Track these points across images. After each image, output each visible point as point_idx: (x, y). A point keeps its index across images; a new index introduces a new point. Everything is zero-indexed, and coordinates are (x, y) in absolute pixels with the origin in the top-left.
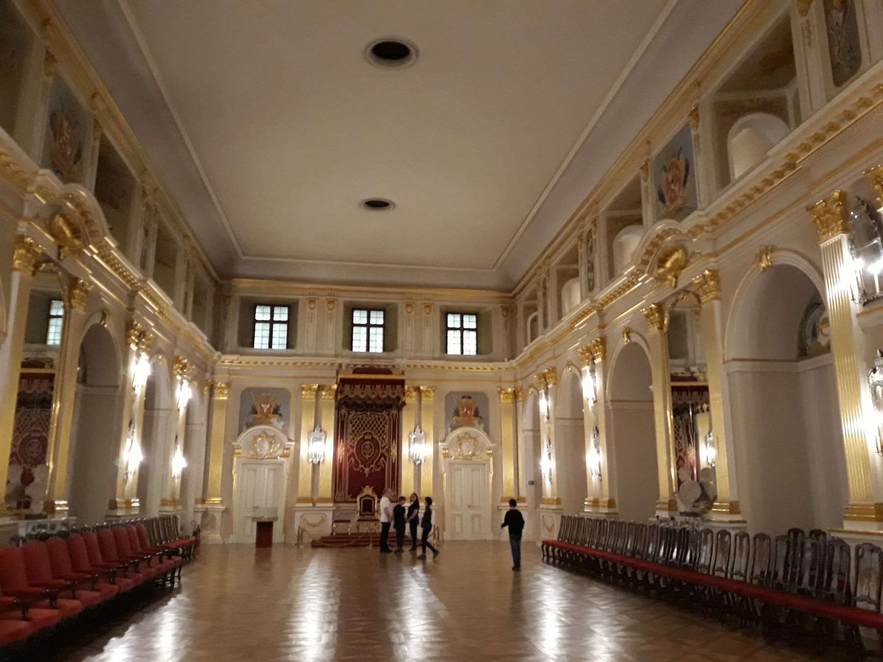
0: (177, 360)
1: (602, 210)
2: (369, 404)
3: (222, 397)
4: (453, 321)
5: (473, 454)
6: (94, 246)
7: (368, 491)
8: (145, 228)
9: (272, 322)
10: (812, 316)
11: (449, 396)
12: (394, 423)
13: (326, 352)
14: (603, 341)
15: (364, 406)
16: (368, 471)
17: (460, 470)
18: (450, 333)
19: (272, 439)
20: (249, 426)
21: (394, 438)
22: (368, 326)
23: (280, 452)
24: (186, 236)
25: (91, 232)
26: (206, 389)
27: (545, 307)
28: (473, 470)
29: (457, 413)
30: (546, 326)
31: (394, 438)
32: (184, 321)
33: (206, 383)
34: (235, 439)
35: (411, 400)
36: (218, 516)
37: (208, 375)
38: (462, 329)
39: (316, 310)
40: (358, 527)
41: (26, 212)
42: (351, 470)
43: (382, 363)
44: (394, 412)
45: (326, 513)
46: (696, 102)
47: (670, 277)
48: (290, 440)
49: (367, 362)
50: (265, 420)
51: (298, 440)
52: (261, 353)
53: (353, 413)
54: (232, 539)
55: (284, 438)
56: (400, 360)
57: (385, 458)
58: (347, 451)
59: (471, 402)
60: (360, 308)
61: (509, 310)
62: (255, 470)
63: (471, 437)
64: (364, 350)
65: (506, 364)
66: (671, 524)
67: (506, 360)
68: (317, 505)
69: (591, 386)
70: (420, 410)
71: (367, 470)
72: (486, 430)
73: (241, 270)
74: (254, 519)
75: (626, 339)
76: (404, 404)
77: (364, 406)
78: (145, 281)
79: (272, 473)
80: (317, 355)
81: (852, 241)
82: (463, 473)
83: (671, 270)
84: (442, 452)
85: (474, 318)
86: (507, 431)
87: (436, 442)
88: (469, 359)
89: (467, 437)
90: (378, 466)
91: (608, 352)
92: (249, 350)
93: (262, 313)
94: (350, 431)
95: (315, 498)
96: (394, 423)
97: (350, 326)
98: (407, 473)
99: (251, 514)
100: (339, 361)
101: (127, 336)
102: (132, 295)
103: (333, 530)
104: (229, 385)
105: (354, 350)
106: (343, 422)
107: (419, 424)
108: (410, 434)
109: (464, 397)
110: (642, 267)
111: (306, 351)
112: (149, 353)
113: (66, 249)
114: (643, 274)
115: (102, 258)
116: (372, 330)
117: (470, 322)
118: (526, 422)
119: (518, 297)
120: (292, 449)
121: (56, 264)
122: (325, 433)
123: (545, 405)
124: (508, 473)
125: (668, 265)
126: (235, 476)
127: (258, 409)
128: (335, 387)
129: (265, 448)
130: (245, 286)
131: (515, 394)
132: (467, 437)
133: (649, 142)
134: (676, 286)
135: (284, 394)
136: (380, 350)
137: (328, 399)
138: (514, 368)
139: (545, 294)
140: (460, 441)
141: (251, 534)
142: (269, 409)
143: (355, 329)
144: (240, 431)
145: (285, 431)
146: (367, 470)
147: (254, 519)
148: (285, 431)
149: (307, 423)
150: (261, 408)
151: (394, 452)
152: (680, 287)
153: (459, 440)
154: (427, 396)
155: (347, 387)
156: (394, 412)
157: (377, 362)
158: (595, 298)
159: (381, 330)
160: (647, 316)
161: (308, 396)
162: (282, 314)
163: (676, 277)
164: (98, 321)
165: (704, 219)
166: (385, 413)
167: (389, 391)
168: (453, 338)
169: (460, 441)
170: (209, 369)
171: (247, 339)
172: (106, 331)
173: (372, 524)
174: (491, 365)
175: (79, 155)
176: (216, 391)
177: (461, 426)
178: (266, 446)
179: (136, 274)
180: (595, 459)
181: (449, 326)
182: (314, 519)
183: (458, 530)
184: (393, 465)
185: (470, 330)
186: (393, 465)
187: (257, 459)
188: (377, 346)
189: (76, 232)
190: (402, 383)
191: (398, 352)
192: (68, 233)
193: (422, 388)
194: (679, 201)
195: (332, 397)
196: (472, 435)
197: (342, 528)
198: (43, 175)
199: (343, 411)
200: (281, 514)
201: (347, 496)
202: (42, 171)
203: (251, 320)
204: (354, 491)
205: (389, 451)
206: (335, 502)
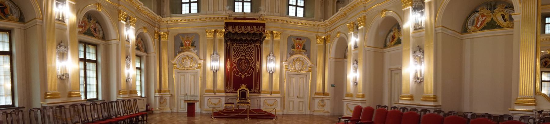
5: (301, 70)
11: (290, 38)
16: (243, 78)
19: (192, 59)
20: (179, 52)
23: (196, 66)
28: (300, 78)
34: (173, 60)
49: (242, 16)
50: (187, 50)
51: (205, 60)
59: (301, 41)
62: (184, 75)
63: (300, 61)
68: (216, 94)
70: (273, 44)
71: (243, 76)
72: (309, 57)
74: (185, 101)
79: (192, 76)
82: (295, 80)
87: (281, 62)
89: (298, 60)
90: (249, 74)
95: (215, 90)
99: (183, 98)
108: (267, 56)
109: (297, 39)
118: (332, 52)
120: (202, 64)
126: (175, 78)
127: (184, 44)
129: (188, 64)
132: (298, 60)
135: (197, 35)
136: (249, 11)
140: (294, 61)
141: (184, 108)
145: (198, 54)
146: (243, 76)
147: (185, 101)
150: (185, 43)
151: (258, 66)
153: (294, 61)
154: (277, 36)
161: (209, 36)
169: (294, 61)
173: (246, 105)
178: (189, 63)
182: (215, 101)
183: (291, 109)
184: (258, 73)
186: (258, 73)
187: (185, 71)
193: (274, 32)
196: (301, 60)
200: (199, 99)
201: (232, 90)
204: (236, 86)
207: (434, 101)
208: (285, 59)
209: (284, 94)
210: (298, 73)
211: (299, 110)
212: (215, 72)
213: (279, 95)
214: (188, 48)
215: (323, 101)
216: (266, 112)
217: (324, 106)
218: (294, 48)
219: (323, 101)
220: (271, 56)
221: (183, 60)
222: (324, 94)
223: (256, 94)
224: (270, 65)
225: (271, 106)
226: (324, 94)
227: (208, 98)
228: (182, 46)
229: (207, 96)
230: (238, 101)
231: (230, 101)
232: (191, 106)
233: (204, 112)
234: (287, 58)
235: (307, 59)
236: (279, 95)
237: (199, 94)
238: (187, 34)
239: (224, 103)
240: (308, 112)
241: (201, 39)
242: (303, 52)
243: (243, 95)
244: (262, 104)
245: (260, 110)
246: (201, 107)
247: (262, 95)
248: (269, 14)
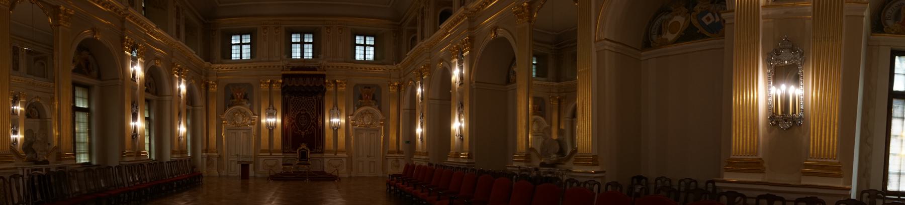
2: (303, 92)
3: (213, 89)
4: (359, 40)
11: (356, 87)
16: (304, 134)
19: (245, 114)
20: (230, 106)
23: (249, 122)
29: (361, 98)
35: (330, 89)
36: (215, 160)
43: (311, 65)
51: (260, 116)
52: (236, 61)
54: (224, 173)
55: (250, 112)
58: (290, 121)
72: (380, 108)
74: (239, 162)
86: (393, 110)
88: (369, 62)
92: (228, 61)
98: (329, 135)
100: (281, 64)
103: (284, 169)
104: (217, 82)
107: (335, 105)
118: (405, 104)
124: (393, 136)
129: (240, 120)
131: (399, 87)
141: (237, 170)
144: (225, 109)
145: (251, 109)
150: (239, 95)
151: (320, 122)
156: (320, 96)
168: (359, 51)
169: (362, 115)
173: (306, 166)
174: (384, 67)
181: (357, 42)
185: (370, 46)
190: (323, 76)
191: (322, 56)
199: (287, 96)
204: (295, 146)
205: (316, 121)
206: (284, 153)
207: (525, 161)
208: (351, 112)
212: (271, 128)
215: (397, 161)
217: (398, 167)
219: (397, 161)
222: (399, 152)
226: (399, 152)
230: (297, 162)
231: (289, 162)
232: (245, 167)
233: (259, 176)
234: (354, 111)
237: (252, 153)
239: (281, 164)
240: (381, 174)
243: (303, 155)
244: (326, 166)
245: (323, 172)
246: (254, 169)
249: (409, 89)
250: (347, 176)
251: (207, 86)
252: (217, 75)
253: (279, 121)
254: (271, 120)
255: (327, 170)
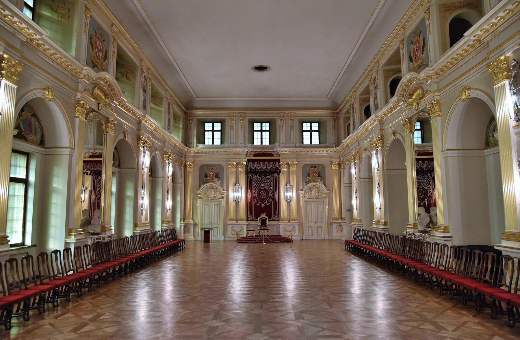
0: (165, 153)
1: (381, 66)
2: (263, 171)
3: (190, 169)
6: (116, 101)
7: (263, 215)
8: (144, 89)
9: (213, 131)
10: (492, 125)
11: (305, 166)
12: (276, 181)
13: (240, 145)
14: (382, 138)
15: (260, 173)
17: (311, 204)
18: (304, 133)
19: (216, 190)
20: (204, 183)
21: (276, 189)
22: (262, 131)
23: (220, 196)
24: (167, 90)
25: (114, 95)
26: (182, 165)
27: (354, 119)
29: (309, 175)
30: (354, 129)
31: (276, 189)
32: (168, 134)
33: (182, 163)
34: (198, 190)
35: (284, 169)
37: (183, 159)
38: (311, 131)
39: (234, 124)
40: (259, 233)
41: (80, 89)
42: (255, 205)
43: (269, 150)
44: (276, 175)
45: (244, 226)
46: (428, 5)
47: (414, 104)
48: (224, 190)
49: (261, 150)
51: (228, 190)
53: (255, 176)
55: (221, 189)
56: (278, 149)
57: (272, 198)
59: (316, 169)
60: (257, 122)
61: (336, 119)
64: (260, 144)
65: (334, 149)
66: (413, 237)
67: (334, 146)
69: (376, 162)
70: (289, 174)
72: (324, 184)
73: (196, 105)
75: (393, 137)
76: (280, 171)
77: (260, 173)
78: (145, 116)
80: (235, 147)
81: (510, 85)
83: (415, 99)
84: (301, 195)
85: (317, 125)
87: (298, 190)
88: (315, 147)
89: (314, 187)
90: (268, 203)
91: (385, 143)
93: (208, 126)
94: (253, 185)
95: (238, 218)
96: (276, 181)
97: (252, 131)
101: (138, 144)
102: (139, 123)
103: (247, 234)
104: (193, 163)
105: (255, 144)
106: (250, 181)
107: (289, 182)
109: (312, 167)
110: (400, 98)
111: (230, 145)
112: (150, 151)
113: (102, 104)
114: (401, 102)
115: (122, 107)
116: (263, 133)
117: (315, 126)
119: (341, 112)
120: (225, 194)
121: (97, 112)
122: (241, 187)
123: (353, 171)
125: (414, 97)
128: (245, 163)
129: (212, 194)
130: (199, 113)
131: (340, 165)
133: (404, 28)
134: (418, 109)
135: (220, 167)
136: (268, 143)
137: (242, 170)
138: (339, 151)
139: (353, 111)
142: (213, 175)
143: (255, 132)
144: (200, 187)
145: (221, 185)
148: (221, 185)
149: (232, 181)
151: (276, 195)
152: (420, 109)
154: (293, 167)
155: (251, 163)
157: (266, 150)
158: (377, 114)
159: (268, 133)
160: (404, 125)
162: (218, 126)
163: (418, 104)
164: (122, 138)
165: (432, 72)
166: (271, 176)
167: (272, 166)
169: (310, 189)
170: (183, 156)
171: (201, 140)
172: (127, 142)
175: (106, 57)
176: (188, 166)
177: (311, 182)
178: (213, 193)
179: (140, 113)
180: (378, 200)
181: (304, 129)
182: (237, 229)
183: (310, 234)
184: (276, 202)
186: (276, 202)
188: (266, 141)
189: (106, 95)
190: (279, 161)
191: (277, 144)
192: (103, 97)
194: (420, 61)
195: (244, 168)
197: (251, 234)
198: (86, 70)
202: (85, 68)
203: (202, 130)
204: (257, 215)
208: (301, 188)
209: (303, 220)
210: (315, 200)
211: (318, 235)
213: (297, 222)
214: (212, 179)
216: (285, 238)
218: (309, 176)
219: (340, 225)
220: (288, 186)
221: (207, 190)
223: (276, 222)
224: (289, 194)
225: (289, 232)
226: (342, 219)
227: (231, 226)
228: (206, 176)
229: (230, 224)
230: (259, 228)
231: (251, 228)
234: (303, 186)
235: (323, 186)
236: (297, 222)
238: (211, 165)
240: (327, 237)
241: (225, 171)
242: (319, 179)
243: (263, 222)
244: (281, 230)
247: (281, 222)
248: (284, 145)
249: (347, 167)
250: (299, 238)
251: (185, 167)
252: (194, 157)
253: (244, 195)
254: (238, 195)
255: (283, 234)
